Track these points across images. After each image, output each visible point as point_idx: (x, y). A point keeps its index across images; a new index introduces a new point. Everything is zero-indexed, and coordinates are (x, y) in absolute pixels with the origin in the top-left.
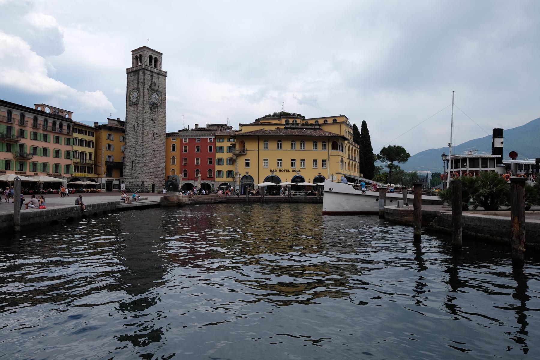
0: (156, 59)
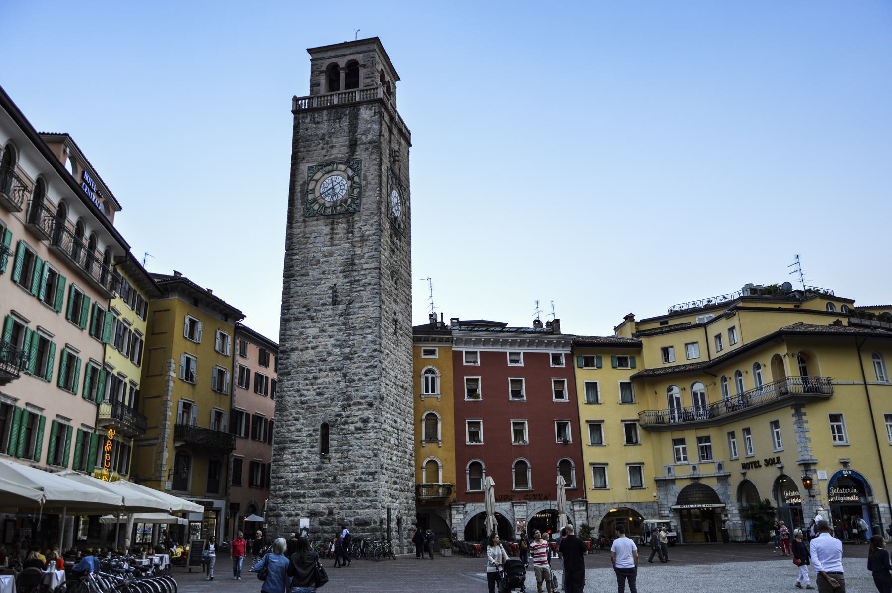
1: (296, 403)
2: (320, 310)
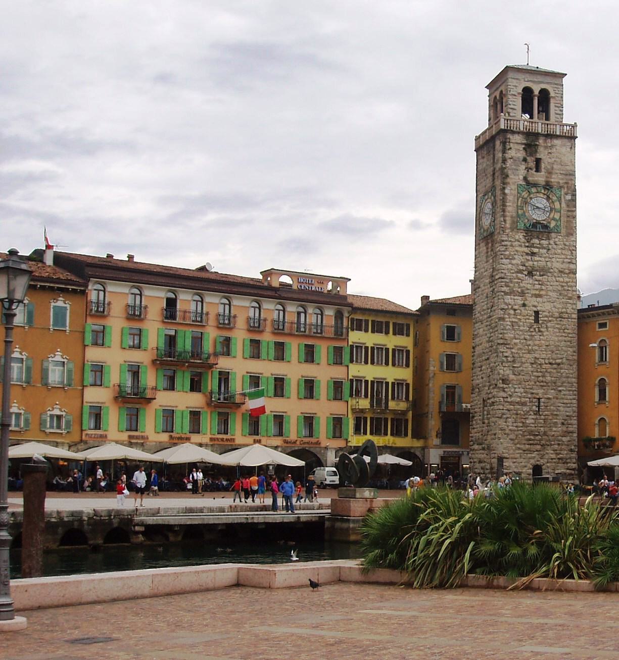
0: (544, 94)
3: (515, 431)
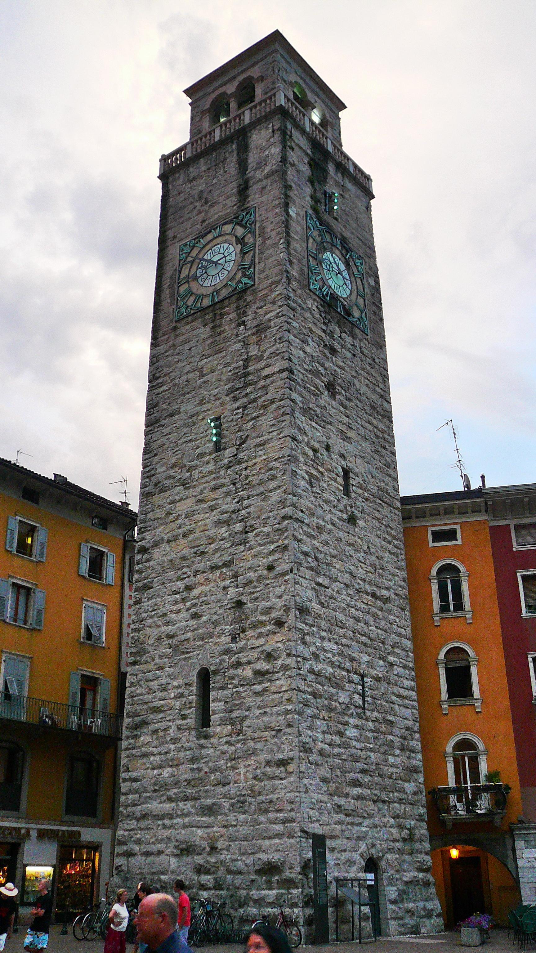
1: (159, 639)
2: (195, 467)
3: (329, 756)
